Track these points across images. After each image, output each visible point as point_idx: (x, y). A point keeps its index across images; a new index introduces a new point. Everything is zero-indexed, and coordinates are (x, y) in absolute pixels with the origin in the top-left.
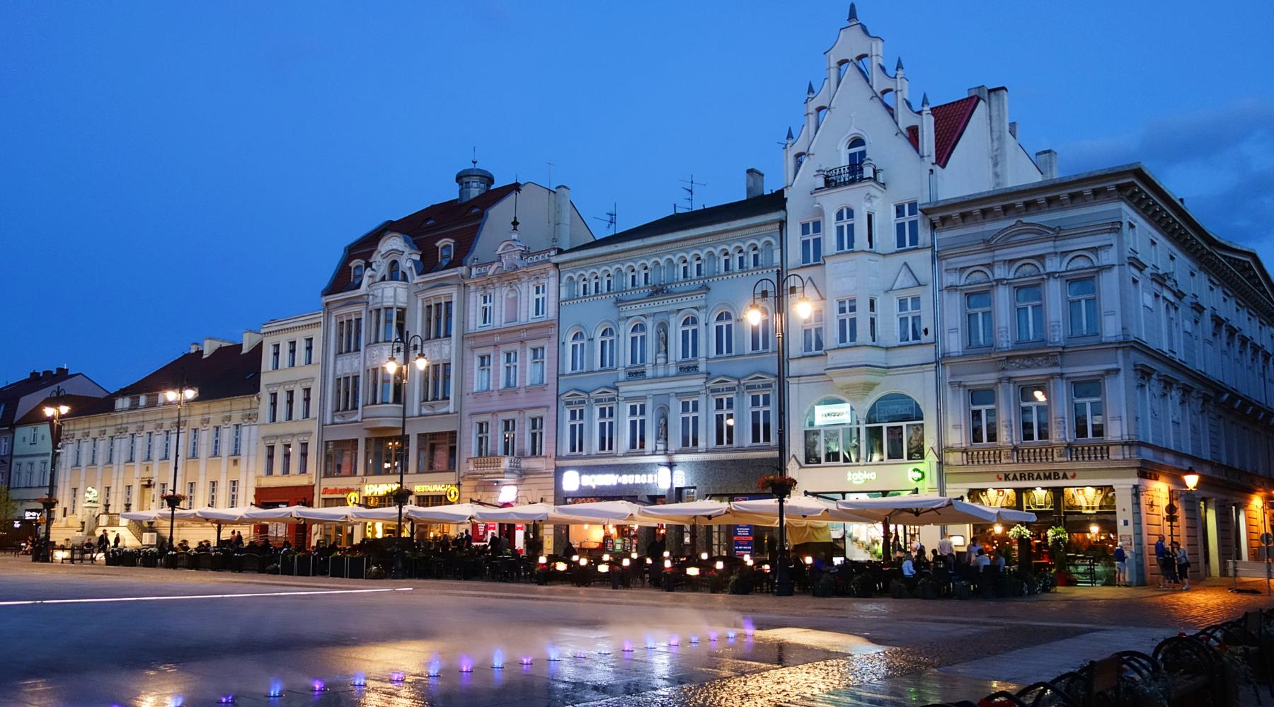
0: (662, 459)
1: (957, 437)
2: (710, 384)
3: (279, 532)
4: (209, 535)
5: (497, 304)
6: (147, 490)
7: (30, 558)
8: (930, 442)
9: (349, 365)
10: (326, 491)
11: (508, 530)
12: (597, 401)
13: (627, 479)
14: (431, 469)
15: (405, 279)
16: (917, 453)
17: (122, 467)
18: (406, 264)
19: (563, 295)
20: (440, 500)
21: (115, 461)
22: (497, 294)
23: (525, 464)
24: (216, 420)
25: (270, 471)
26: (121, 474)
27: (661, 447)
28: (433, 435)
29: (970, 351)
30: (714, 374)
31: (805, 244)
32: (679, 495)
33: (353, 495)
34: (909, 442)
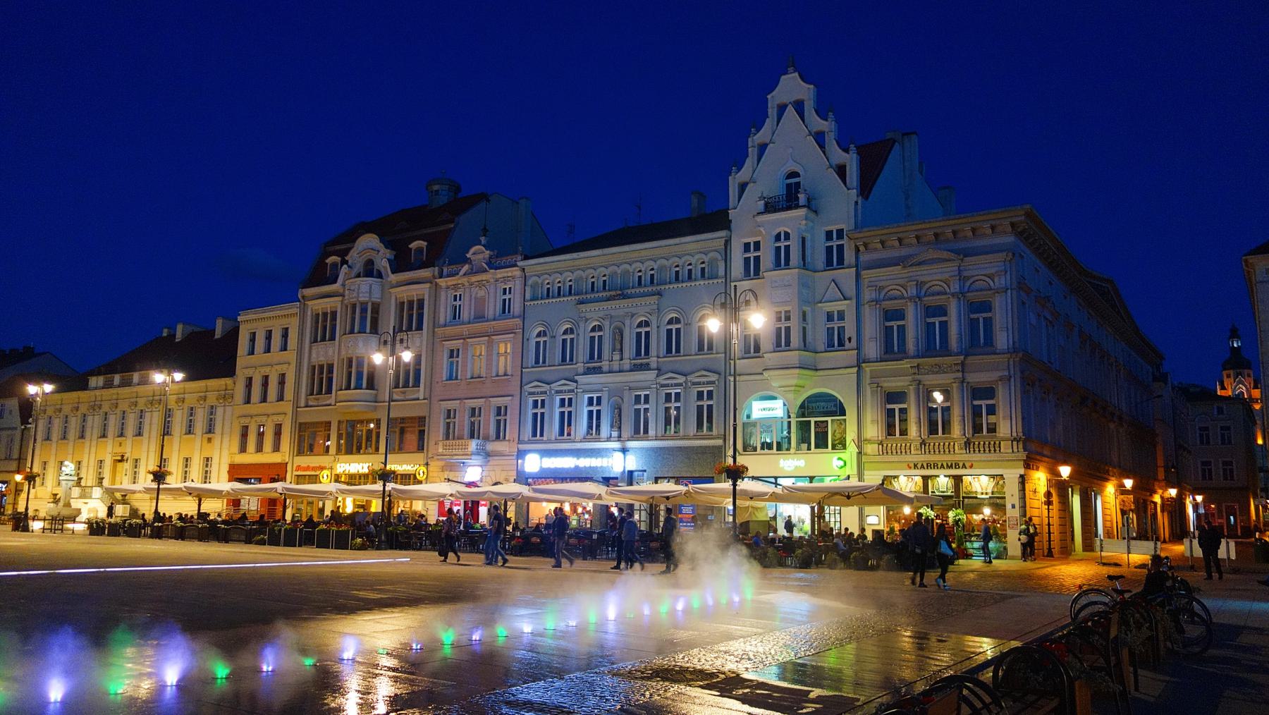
0: (616, 445)
1: (873, 430)
2: (661, 380)
3: (251, 506)
4: (188, 507)
5: (467, 303)
6: (120, 465)
7: (9, 527)
8: (851, 435)
9: (324, 353)
10: (299, 468)
11: (472, 507)
12: (557, 392)
13: (584, 462)
14: (401, 450)
15: (380, 276)
16: (841, 444)
17: (94, 443)
18: (383, 263)
19: (528, 296)
20: (408, 478)
21: (88, 434)
22: (467, 295)
23: (491, 446)
24: (191, 400)
25: (243, 449)
26: (93, 450)
27: (615, 434)
28: (403, 419)
29: (888, 356)
30: (664, 368)
31: (747, 260)
32: (630, 477)
33: (326, 472)
34: (833, 435)
